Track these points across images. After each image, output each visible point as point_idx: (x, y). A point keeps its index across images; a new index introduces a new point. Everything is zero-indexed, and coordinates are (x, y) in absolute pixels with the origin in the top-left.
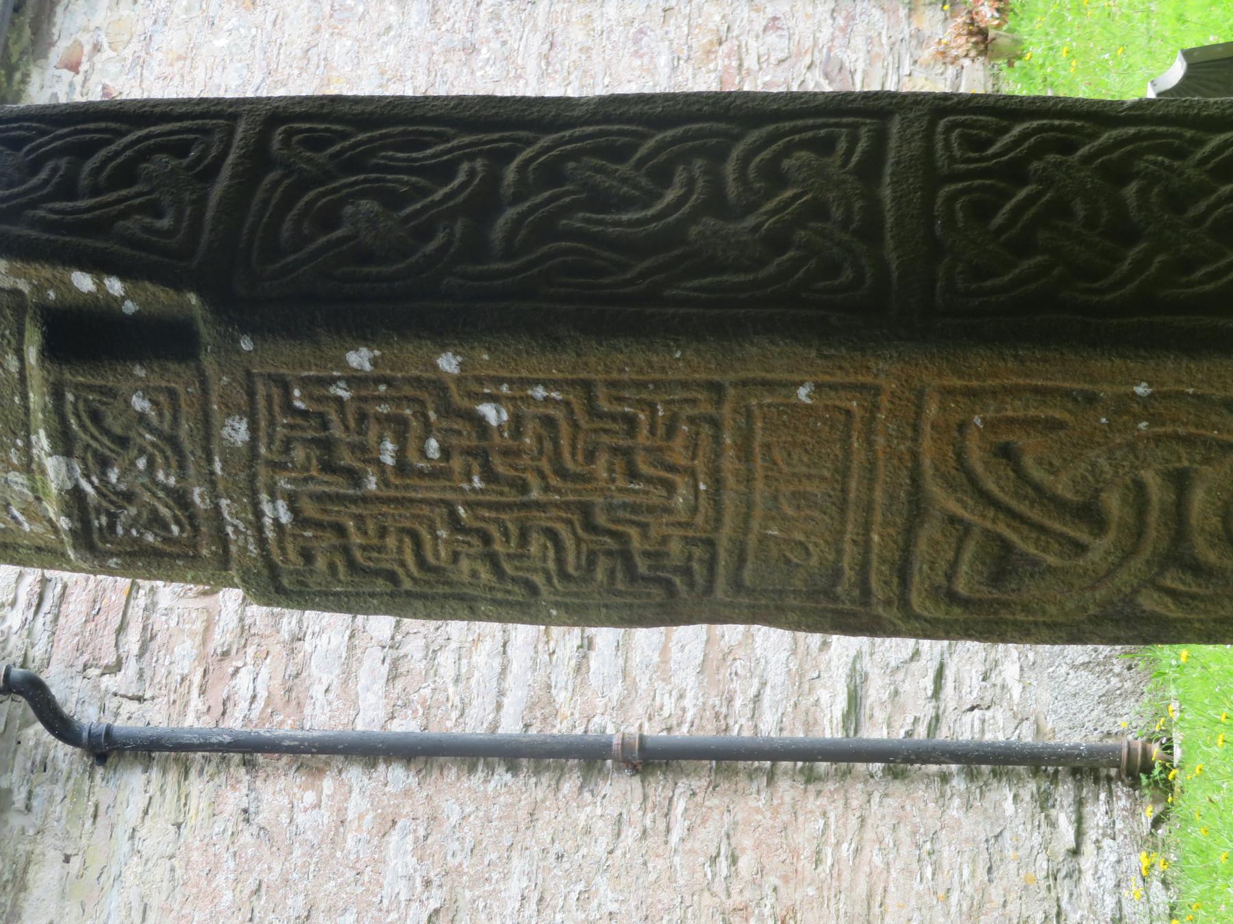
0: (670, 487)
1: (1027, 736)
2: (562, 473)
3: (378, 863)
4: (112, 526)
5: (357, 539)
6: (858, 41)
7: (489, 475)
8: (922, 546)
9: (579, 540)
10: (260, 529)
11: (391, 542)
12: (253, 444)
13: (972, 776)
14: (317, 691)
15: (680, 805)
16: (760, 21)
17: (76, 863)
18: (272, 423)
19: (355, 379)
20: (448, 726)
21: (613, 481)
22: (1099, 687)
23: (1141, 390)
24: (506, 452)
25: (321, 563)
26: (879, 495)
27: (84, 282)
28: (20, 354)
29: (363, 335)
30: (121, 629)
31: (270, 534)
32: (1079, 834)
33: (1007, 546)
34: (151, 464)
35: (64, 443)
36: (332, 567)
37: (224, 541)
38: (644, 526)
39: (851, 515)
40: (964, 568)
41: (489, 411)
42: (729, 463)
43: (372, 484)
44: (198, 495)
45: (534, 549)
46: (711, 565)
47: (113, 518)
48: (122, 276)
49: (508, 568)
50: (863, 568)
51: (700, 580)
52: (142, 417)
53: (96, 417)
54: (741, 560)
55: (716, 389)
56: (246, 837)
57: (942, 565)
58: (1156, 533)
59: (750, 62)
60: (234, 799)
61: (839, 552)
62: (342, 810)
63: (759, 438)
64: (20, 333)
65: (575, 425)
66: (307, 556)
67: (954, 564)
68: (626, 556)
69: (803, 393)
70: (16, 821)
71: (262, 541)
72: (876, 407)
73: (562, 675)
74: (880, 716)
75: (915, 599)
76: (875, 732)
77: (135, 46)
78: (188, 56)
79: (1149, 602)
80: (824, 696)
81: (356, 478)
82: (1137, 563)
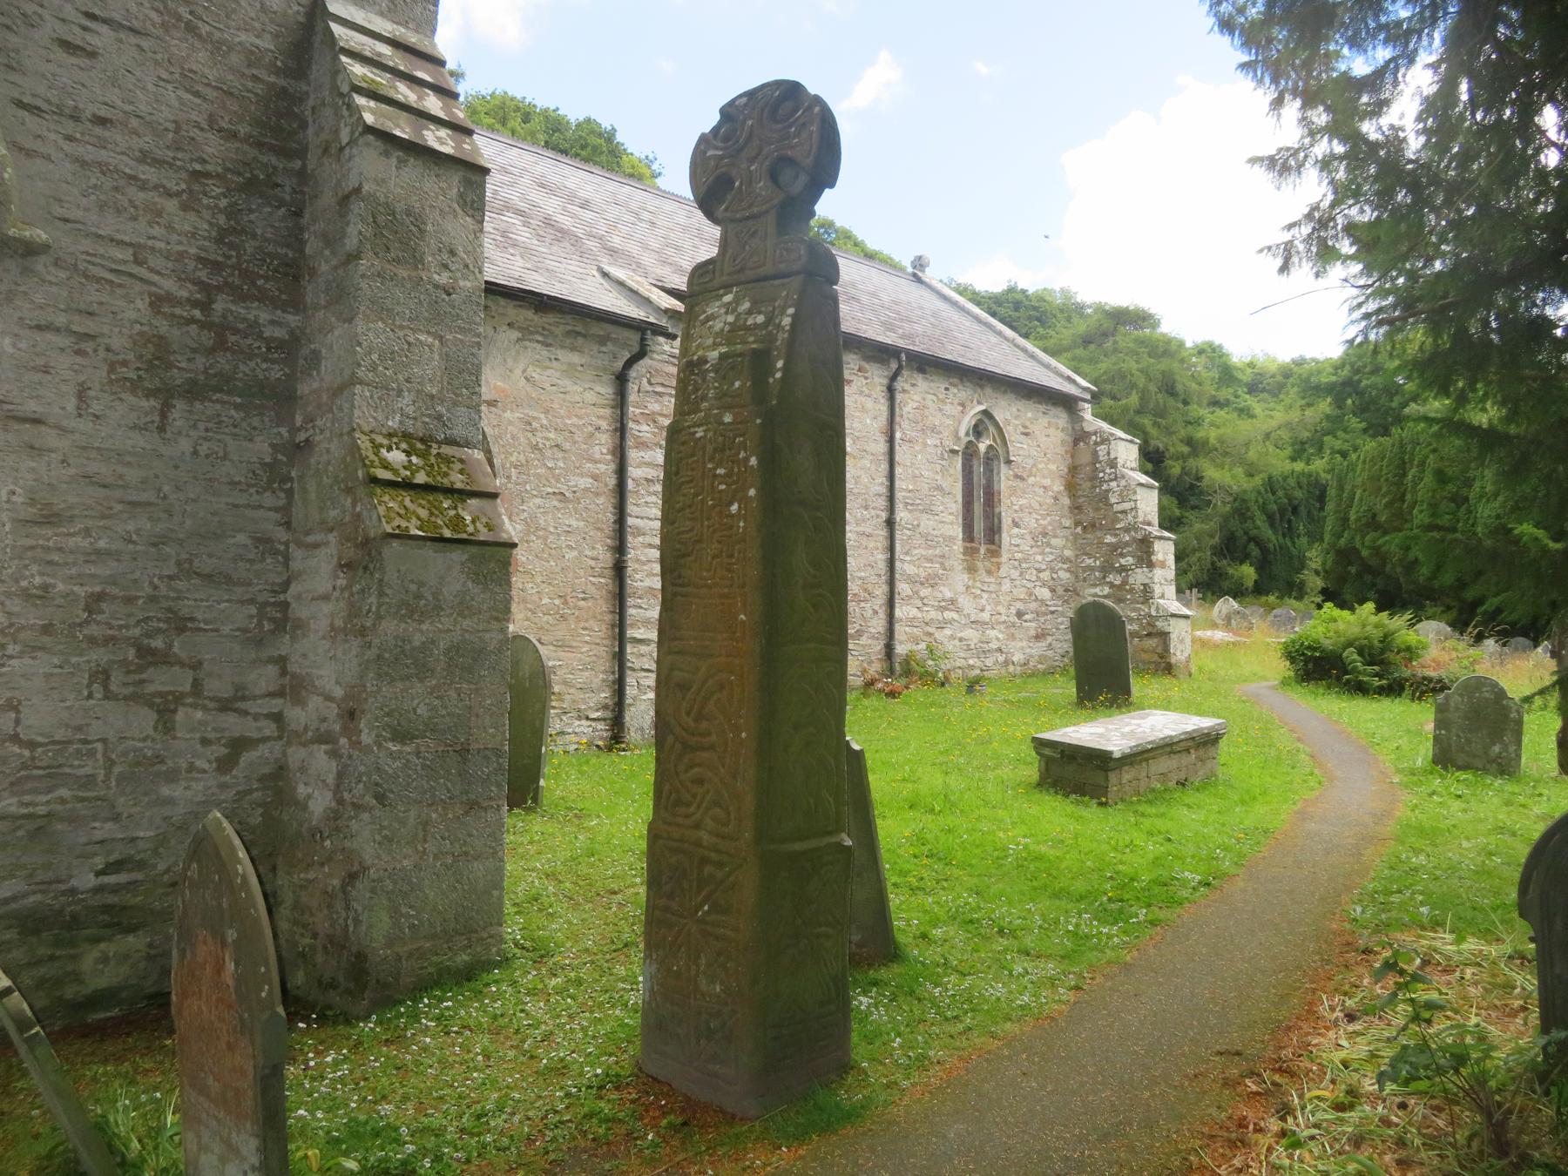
0: (708, 571)
1: (628, 701)
2: (714, 532)
3: (582, 475)
5: (690, 461)
6: (869, 642)
7: (714, 506)
10: (694, 426)
11: (689, 473)
12: (723, 424)
13: (614, 682)
14: (642, 454)
15: (602, 580)
16: (877, 608)
17: (580, 368)
19: (747, 459)
20: (630, 500)
22: (646, 726)
23: (744, 735)
24: (721, 512)
25: (682, 448)
27: (780, 364)
28: (754, 342)
29: (760, 462)
30: (663, 385)
31: (692, 430)
32: (594, 720)
33: (688, 690)
34: (716, 388)
35: (722, 357)
38: (695, 561)
41: (734, 508)
43: (710, 466)
44: (705, 405)
45: (688, 523)
46: (681, 586)
48: (782, 378)
54: (683, 596)
55: (743, 586)
56: (590, 429)
59: (862, 604)
60: (604, 424)
62: (600, 462)
64: (762, 342)
66: (683, 443)
68: (683, 556)
69: (743, 617)
70: (595, 348)
71: (689, 427)
73: (648, 539)
74: (635, 650)
76: (629, 649)
77: (867, 392)
78: (864, 409)
79: (670, 739)
80: (642, 631)
81: (711, 459)
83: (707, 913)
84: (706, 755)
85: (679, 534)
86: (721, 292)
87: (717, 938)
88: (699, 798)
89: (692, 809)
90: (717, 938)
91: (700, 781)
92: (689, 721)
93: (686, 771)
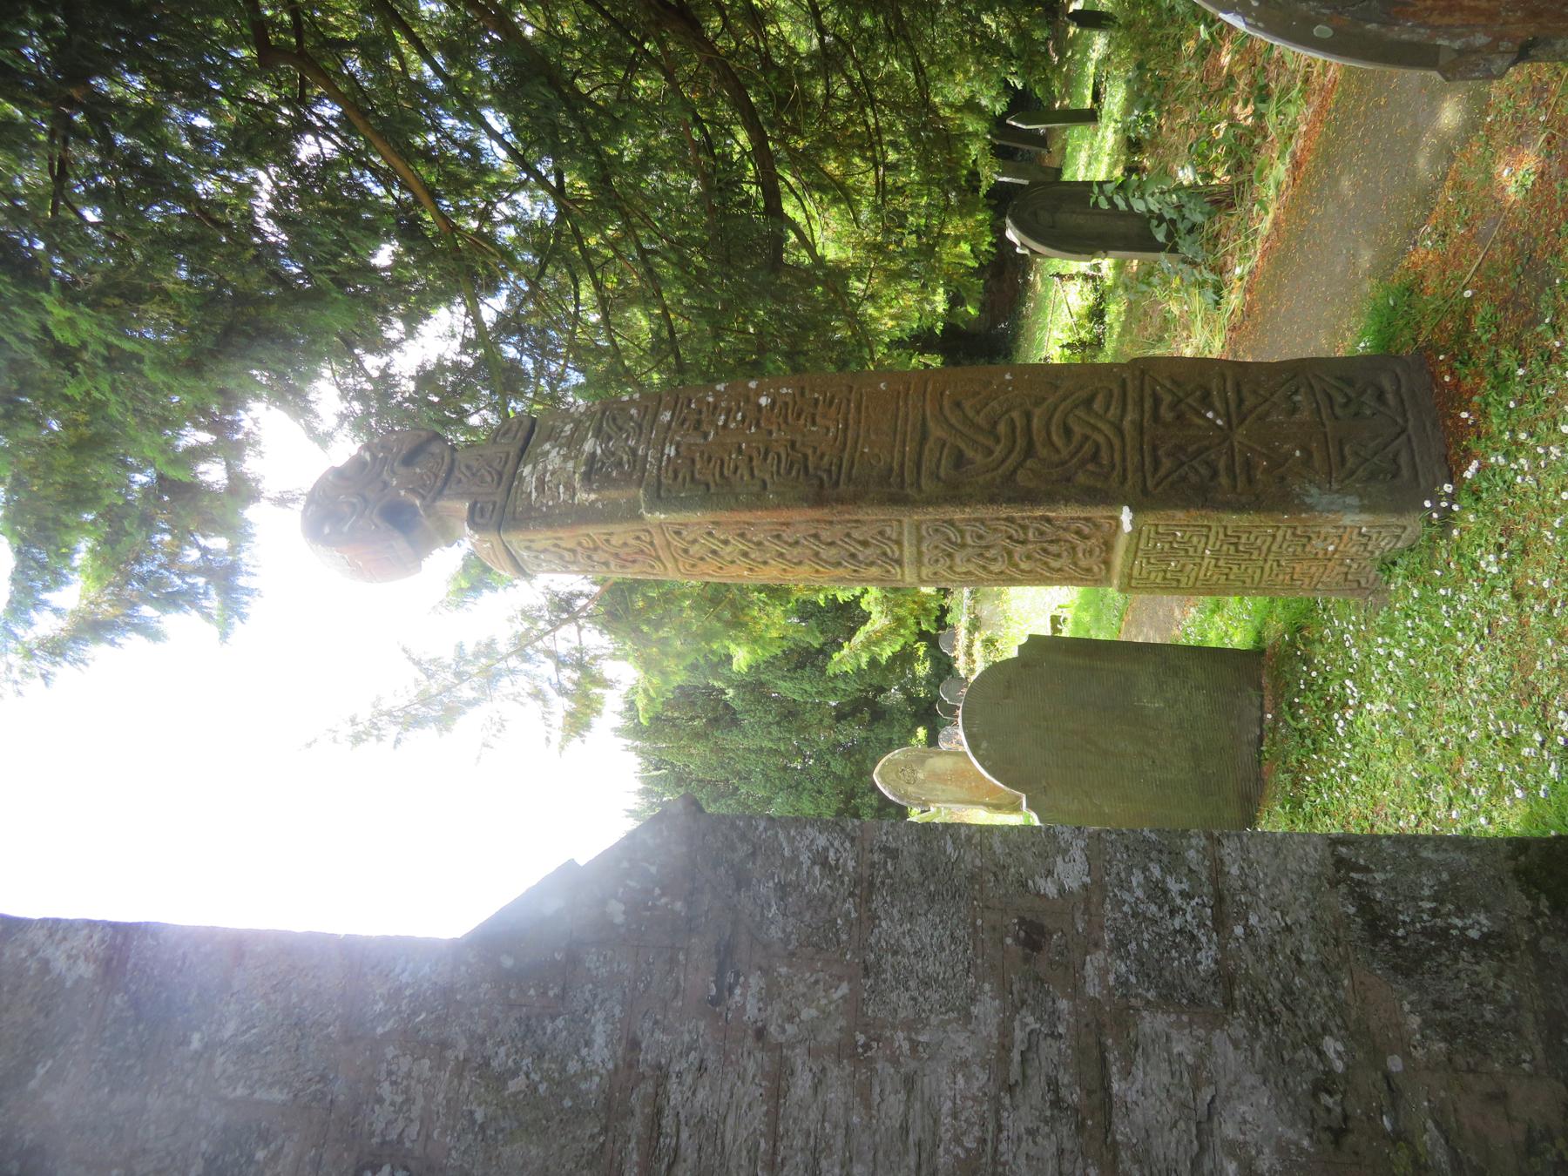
2: (786, 422)
4: (601, 468)
8: (926, 452)
9: (788, 455)
10: (661, 462)
18: (681, 412)
21: (805, 426)
26: (909, 428)
35: (596, 436)
36: (684, 478)
37: (644, 470)
39: (898, 437)
40: (943, 462)
41: (763, 401)
42: (851, 416)
47: (603, 464)
49: (756, 472)
50: (902, 466)
51: (834, 477)
52: (631, 417)
53: (614, 419)
57: (935, 460)
58: (1021, 443)
61: (893, 458)
63: (864, 404)
65: (795, 403)
67: (939, 460)
71: (659, 468)
72: (909, 389)
75: (923, 482)
82: (1014, 455)
83: (1217, 414)
84: (1035, 422)
85: (778, 472)
86: (516, 483)
87: (1241, 401)
88: (1088, 431)
89: (1101, 439)
90: (1241, 401)
91: (1067, 432)
92: (999, 450)
93: (1057, 451)
